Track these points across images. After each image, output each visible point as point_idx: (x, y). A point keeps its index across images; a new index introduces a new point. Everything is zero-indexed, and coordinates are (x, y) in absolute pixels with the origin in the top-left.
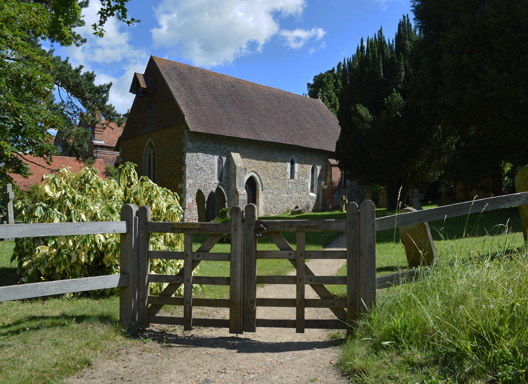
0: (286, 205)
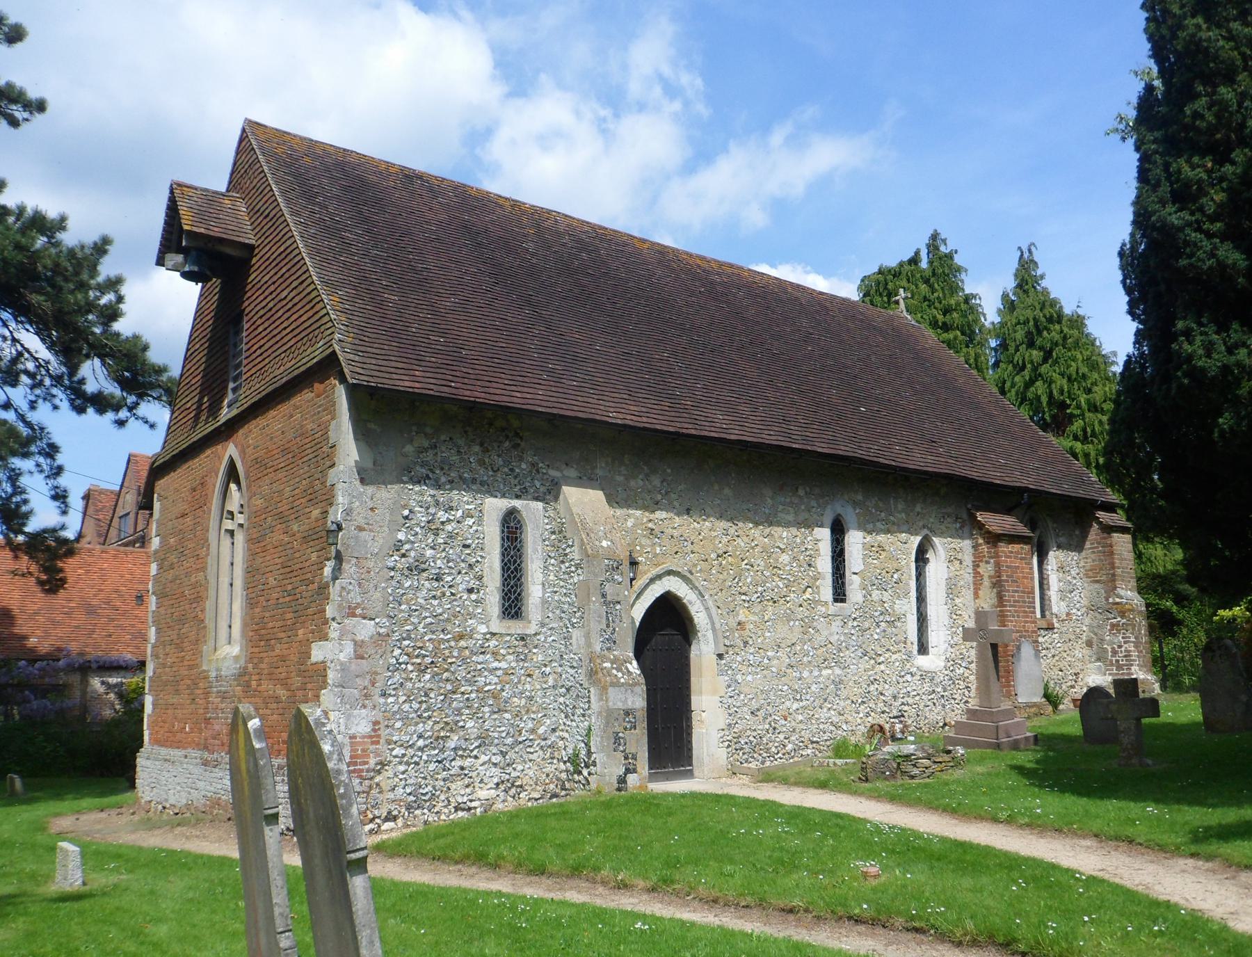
0: (823, 714)
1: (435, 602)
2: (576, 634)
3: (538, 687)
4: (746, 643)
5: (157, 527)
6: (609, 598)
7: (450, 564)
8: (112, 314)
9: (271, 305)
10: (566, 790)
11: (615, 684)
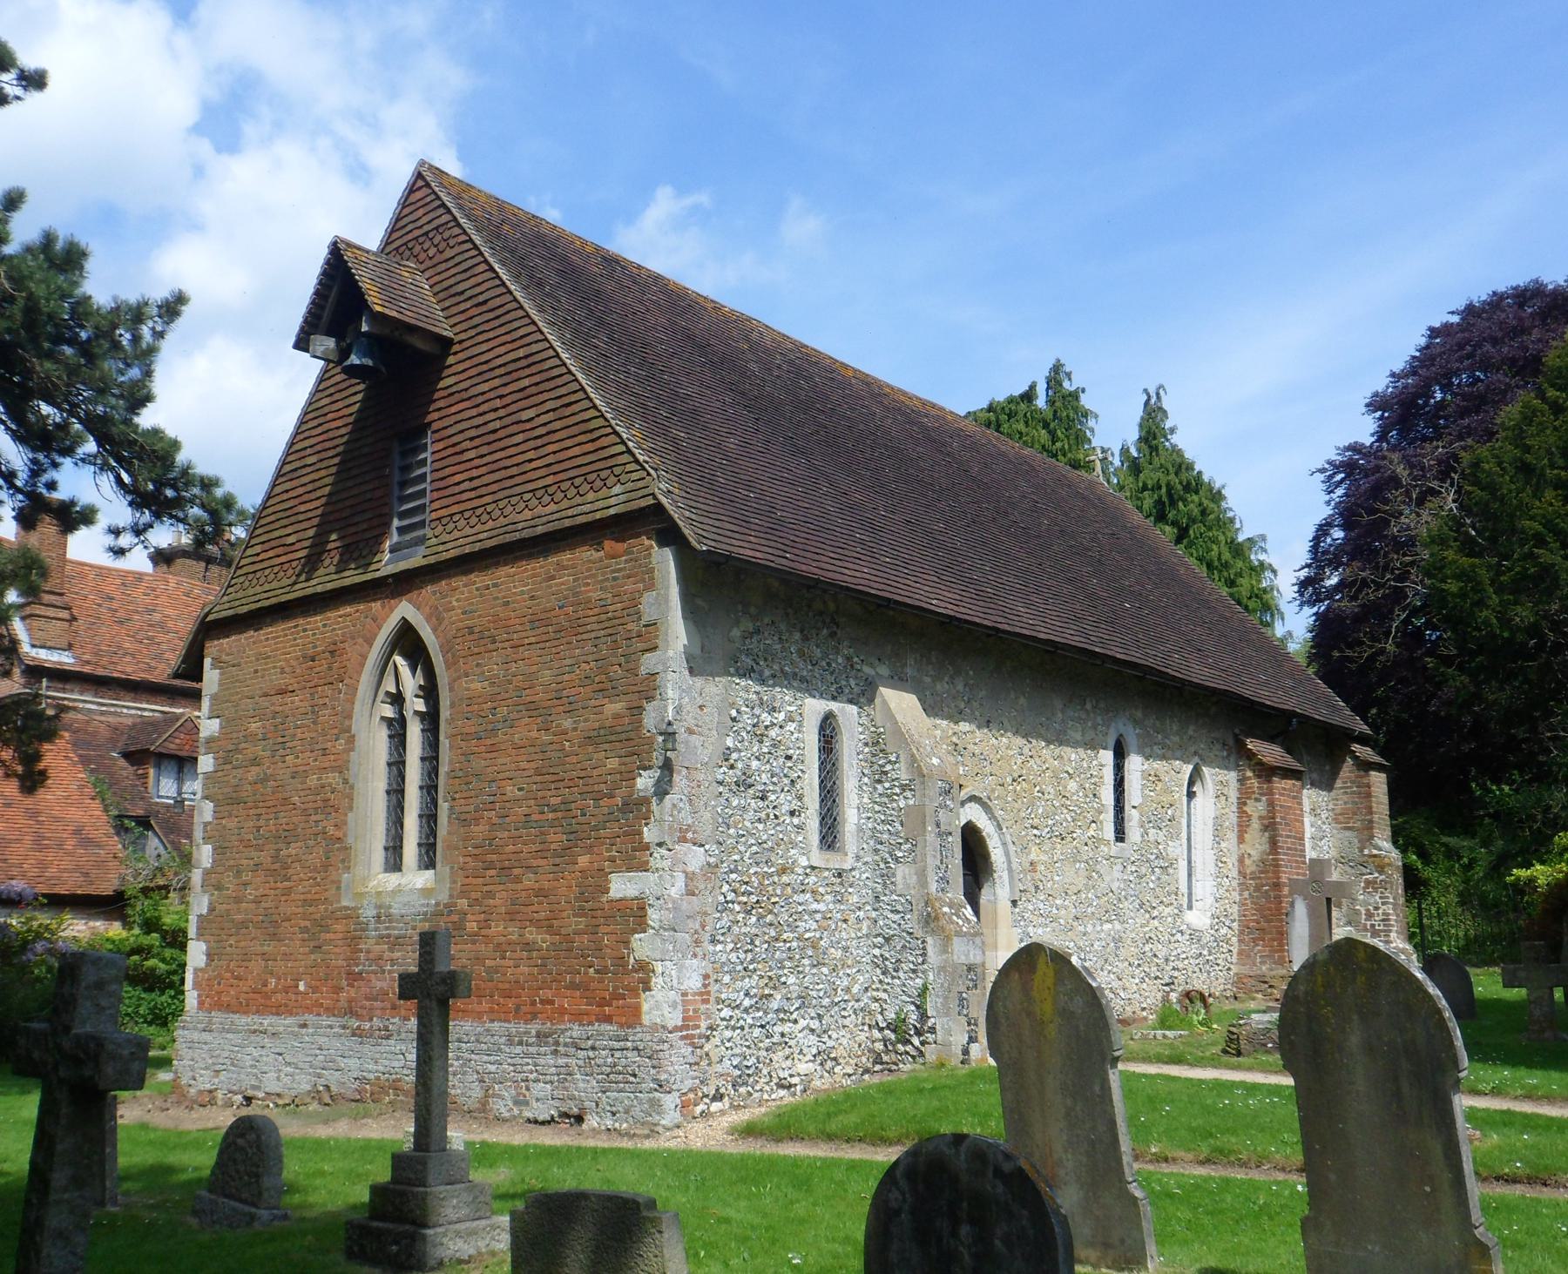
1: (761, 826)
2: (904, 874)
3: (853, 935)
4: (1037, 888)
5: (212, 705)
6: (943, 828)
7: (775, 779)
8: (139, 397)
9: (497, 424)
10: (882, 1063)
11: (959, 934)
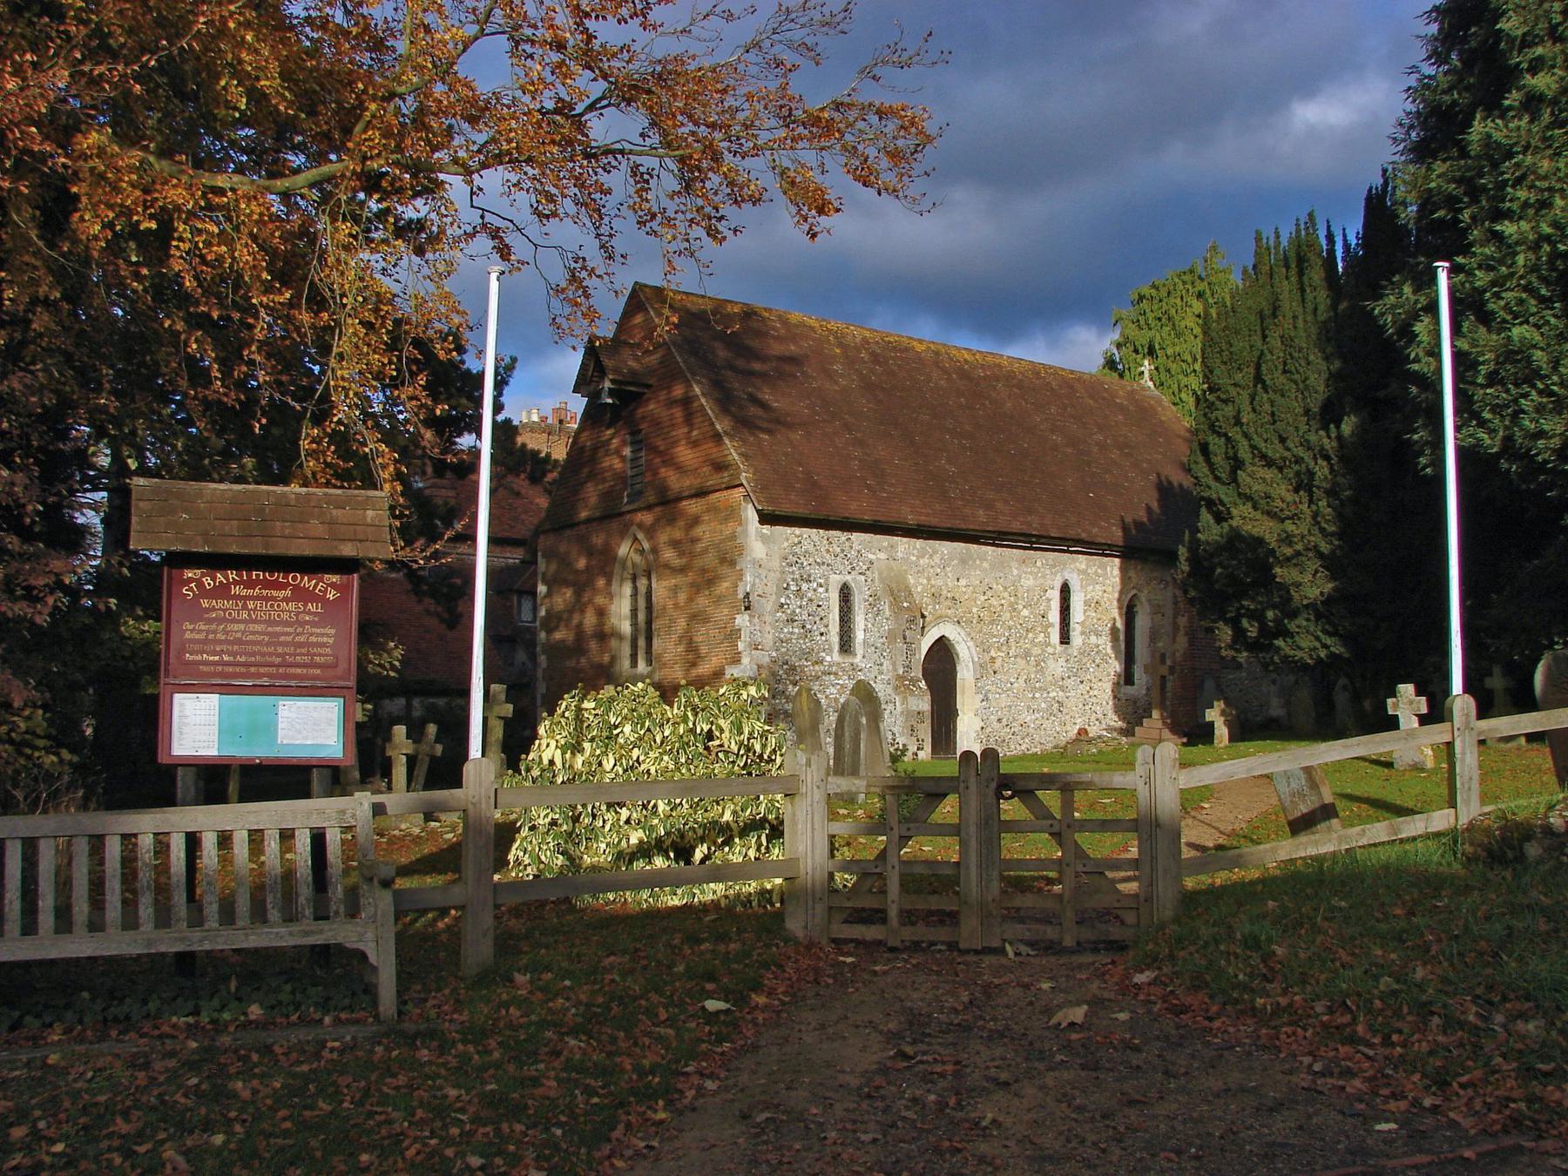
2: (886, 664)
